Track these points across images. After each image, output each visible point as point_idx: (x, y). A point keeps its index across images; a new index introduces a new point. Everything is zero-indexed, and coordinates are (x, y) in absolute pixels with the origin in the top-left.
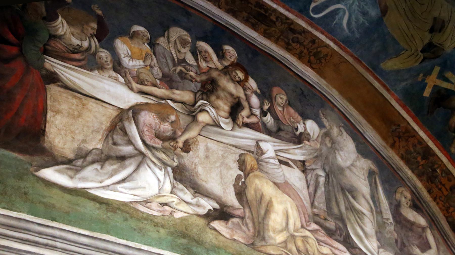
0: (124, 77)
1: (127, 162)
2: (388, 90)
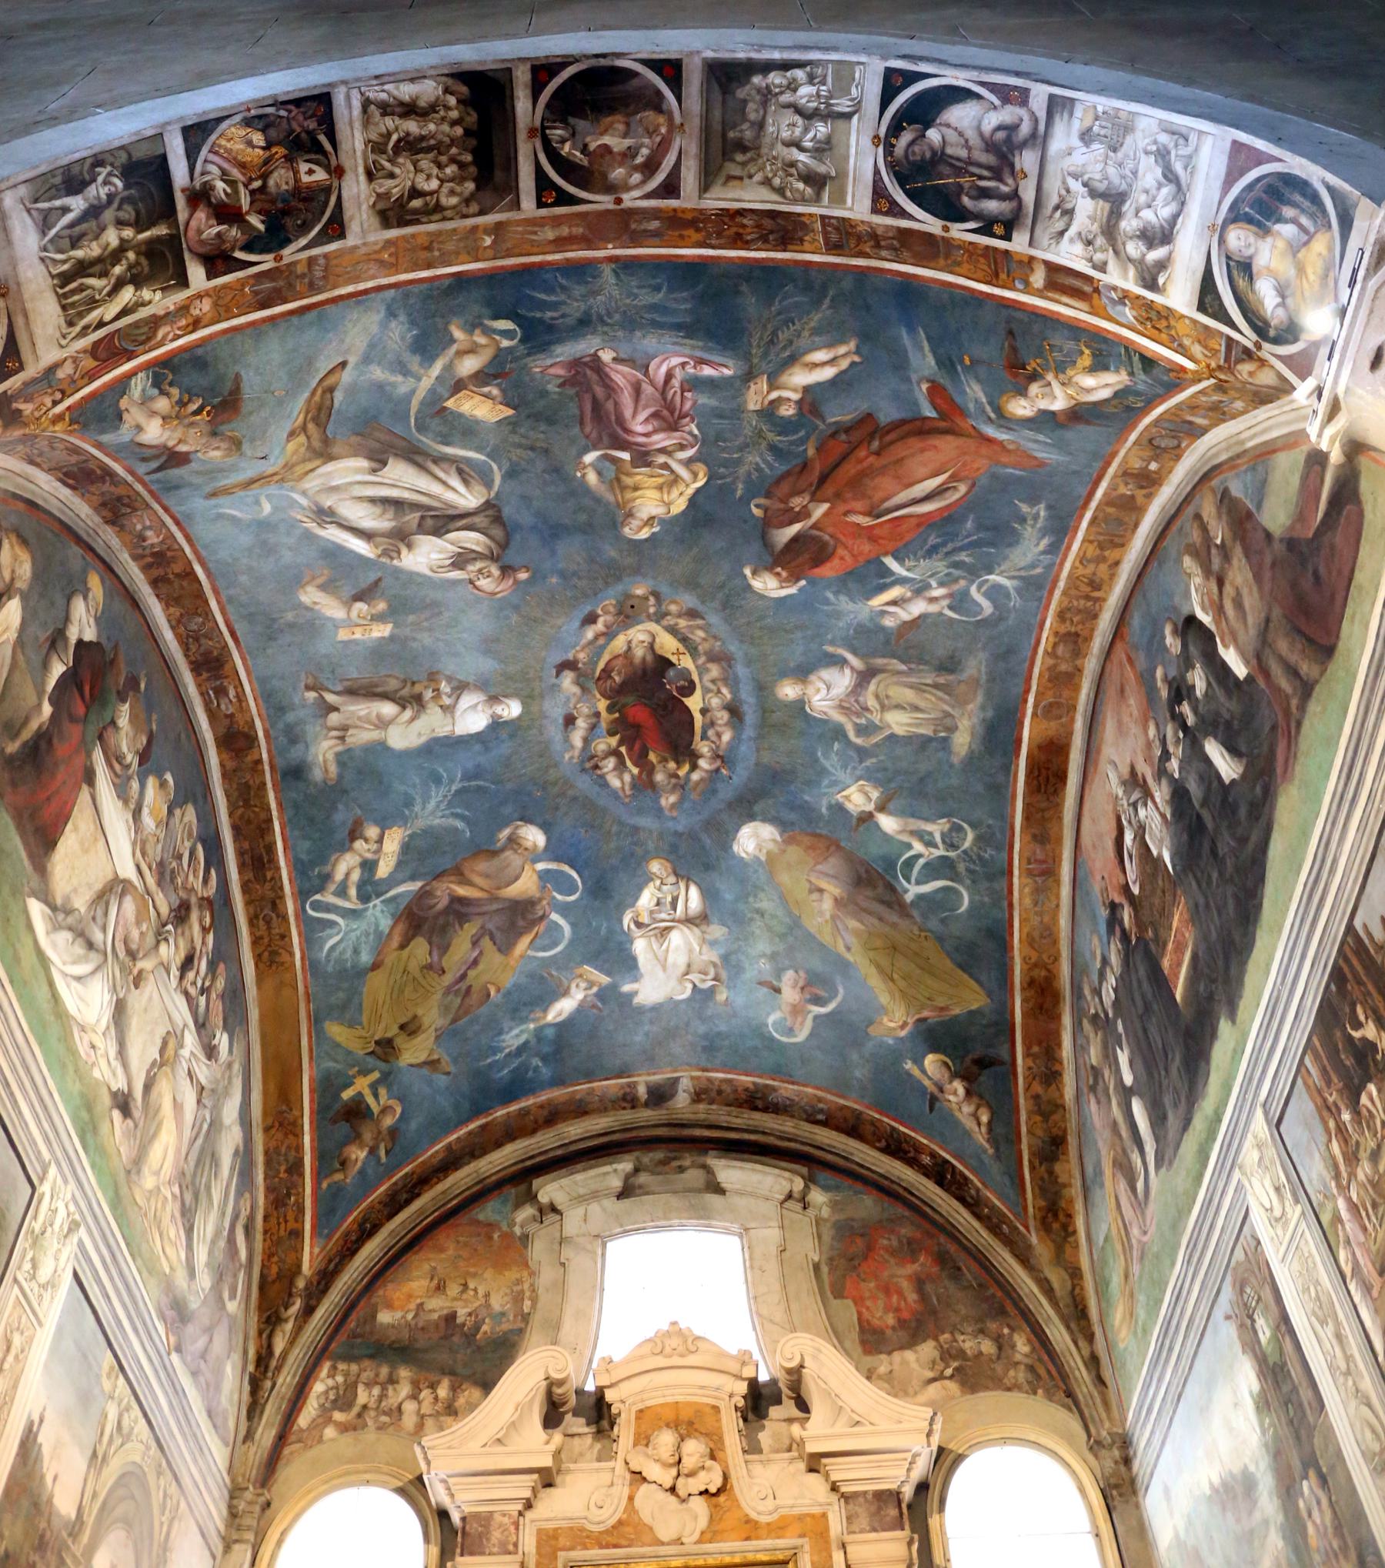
1: (93, 955)
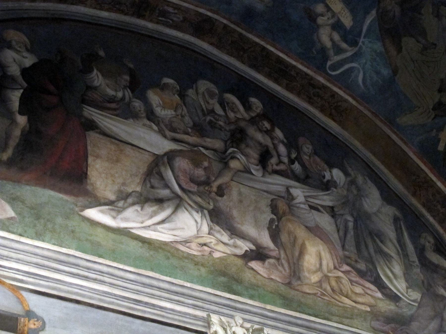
0: (158, 125)
1: (165, 205)
2: (405, 143)
